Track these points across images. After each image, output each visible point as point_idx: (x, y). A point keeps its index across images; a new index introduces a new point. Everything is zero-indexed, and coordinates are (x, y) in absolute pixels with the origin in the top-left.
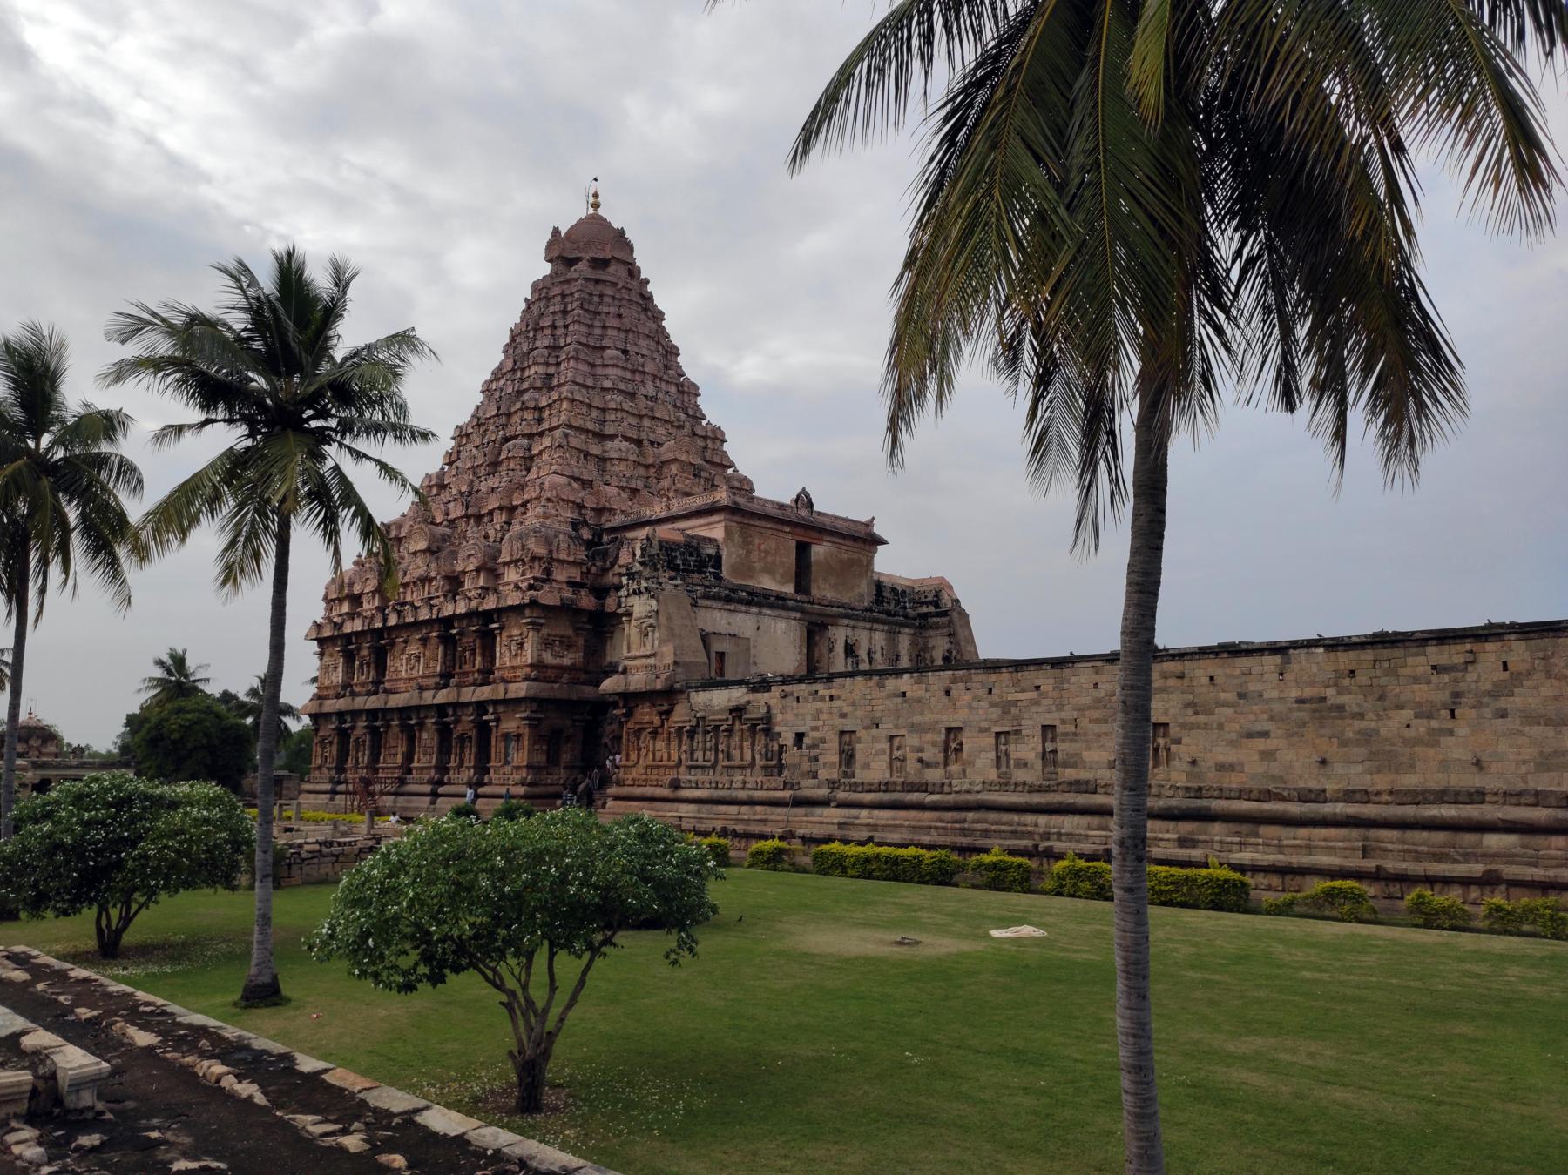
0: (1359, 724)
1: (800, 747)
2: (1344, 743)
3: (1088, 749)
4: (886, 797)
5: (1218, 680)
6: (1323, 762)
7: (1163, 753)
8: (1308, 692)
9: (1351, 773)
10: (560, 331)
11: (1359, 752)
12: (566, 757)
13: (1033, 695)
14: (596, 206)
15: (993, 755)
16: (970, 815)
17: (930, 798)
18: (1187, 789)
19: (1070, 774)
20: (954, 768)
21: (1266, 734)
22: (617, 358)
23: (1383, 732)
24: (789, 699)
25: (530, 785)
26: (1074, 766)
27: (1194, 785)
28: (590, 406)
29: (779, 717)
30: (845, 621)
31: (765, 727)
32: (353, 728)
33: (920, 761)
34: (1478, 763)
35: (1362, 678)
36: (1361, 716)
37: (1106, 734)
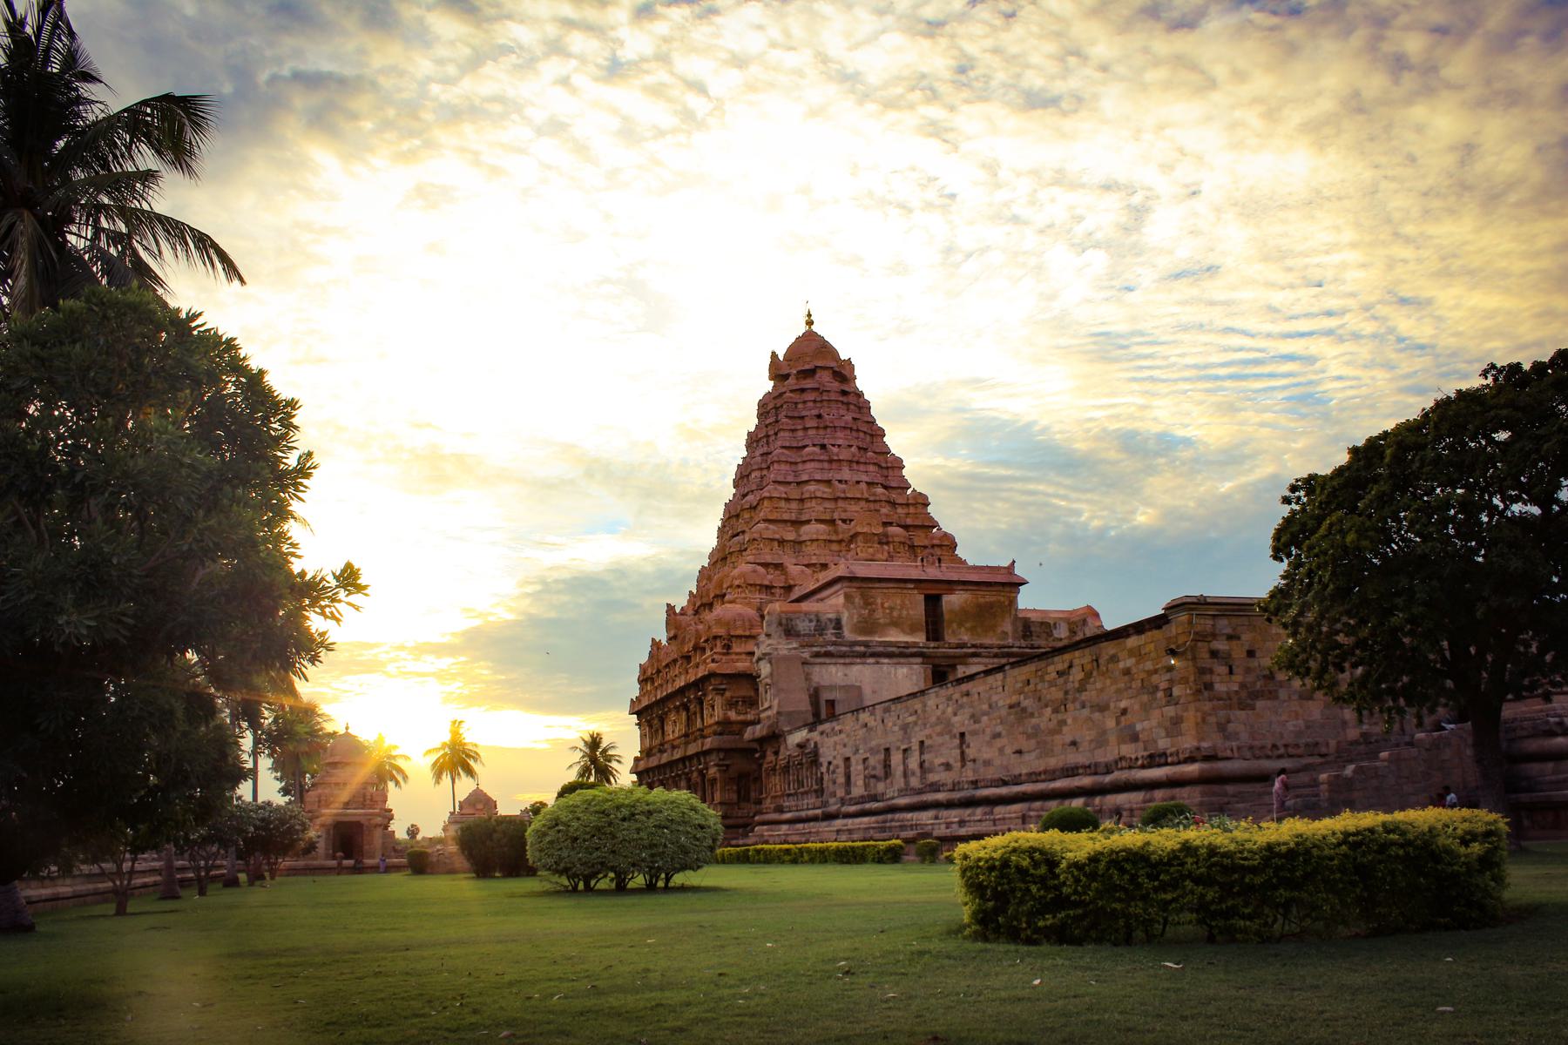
0: (1034, 721)
2: (1029, 737)
6: (1019, 752)
8: (1014, 699)
11: (1033, 742)
14: (810, 323)
16: (889, 816)
17: (875, 805)
22: (813, 453)
23: (1042, 726)
28: (787, 500)
30: (975, 660)
31: (815, 760)
33: (874, 777)
34: (1074, 743)
36: (1032, 715)
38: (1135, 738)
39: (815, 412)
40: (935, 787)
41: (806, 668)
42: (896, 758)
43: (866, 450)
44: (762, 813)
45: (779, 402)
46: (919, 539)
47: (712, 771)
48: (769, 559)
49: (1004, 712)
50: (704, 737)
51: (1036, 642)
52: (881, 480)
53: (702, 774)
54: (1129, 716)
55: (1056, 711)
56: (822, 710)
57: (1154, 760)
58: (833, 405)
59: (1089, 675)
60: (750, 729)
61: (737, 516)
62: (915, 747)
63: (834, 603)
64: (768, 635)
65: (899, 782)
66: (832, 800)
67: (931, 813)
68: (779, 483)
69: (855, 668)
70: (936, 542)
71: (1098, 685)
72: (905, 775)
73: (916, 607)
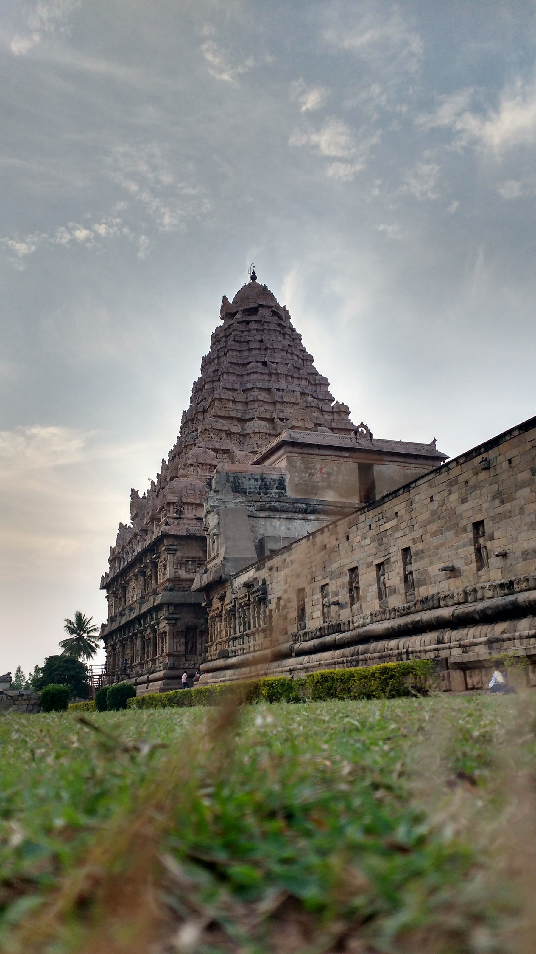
1: (279, 611)
3: (431, 563)
4: (316, 641)
5: (515, 462)
7: (484, 553)
13: (393, 523)
14: (254, 278)
15: (375, 587)
16: (361, 648)
18: (502, 586)
19: (423, 592)
20: (355, 607)
22: (257, 367)
24: (275, 569)
25: (170, 668)
26: (424, 584)
27: (506, 581)
28: (234, 402)
29: (269, 587)
31: (263, 598)
32: (116, 644)
33: (336, 604)
37: (442, 545)
41: (252, 521)
42: (367, 578)
43: (299, 369)
44: (205, 661)
58: (273, 333)
62: (397, 557)
65: (371, 603)
67: (431, 636)
72: (381, 595)
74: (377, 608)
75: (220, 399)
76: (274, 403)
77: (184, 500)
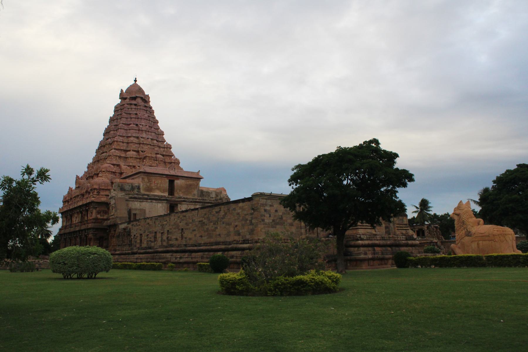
0: (207, 227)
6: (201, 236)
8: (201, 219)
9: (205, 239)
10: (119, 120)
12: (104, 244)
15: (160, 239)
16: (155, 254)
19: (171, 242)
21: (195, 230)
22: (133, 127)
28: (123, 142)
30: (184, 203)
31: (129, 234)
34: (219, 235)
35: (207, 216)
36: (206, 225)
38: (239, 234)
39: (135, 112)
40: (172, 246)
42: (159, 235)
43: (151, 127)
45: (122, 107)
46: (167, 160)
47: (90, 236)
48: (115, 163)
49: (197, 223)
50: (88, 223)
51: (205, 198)
52: (156, 138)
53: (86, 236)
54: (238, 227)
55: (214, 224)
56: (132, 217)
57: (245, 242)
59: (226, 214)
60: (106, 222)
61: (104, 146)
62: (166, 232)
63: (137, 181)
64: (114, 190)
65: (159, 243)
66: (134, 248)
68: (121, 136)
69: (144, 203)
70: (173, 161)
71: (229, 217)
73: (165, 184)
74: (160, 244)
75: (117, 141)
76: (140, 144)
77: (101, 188)
